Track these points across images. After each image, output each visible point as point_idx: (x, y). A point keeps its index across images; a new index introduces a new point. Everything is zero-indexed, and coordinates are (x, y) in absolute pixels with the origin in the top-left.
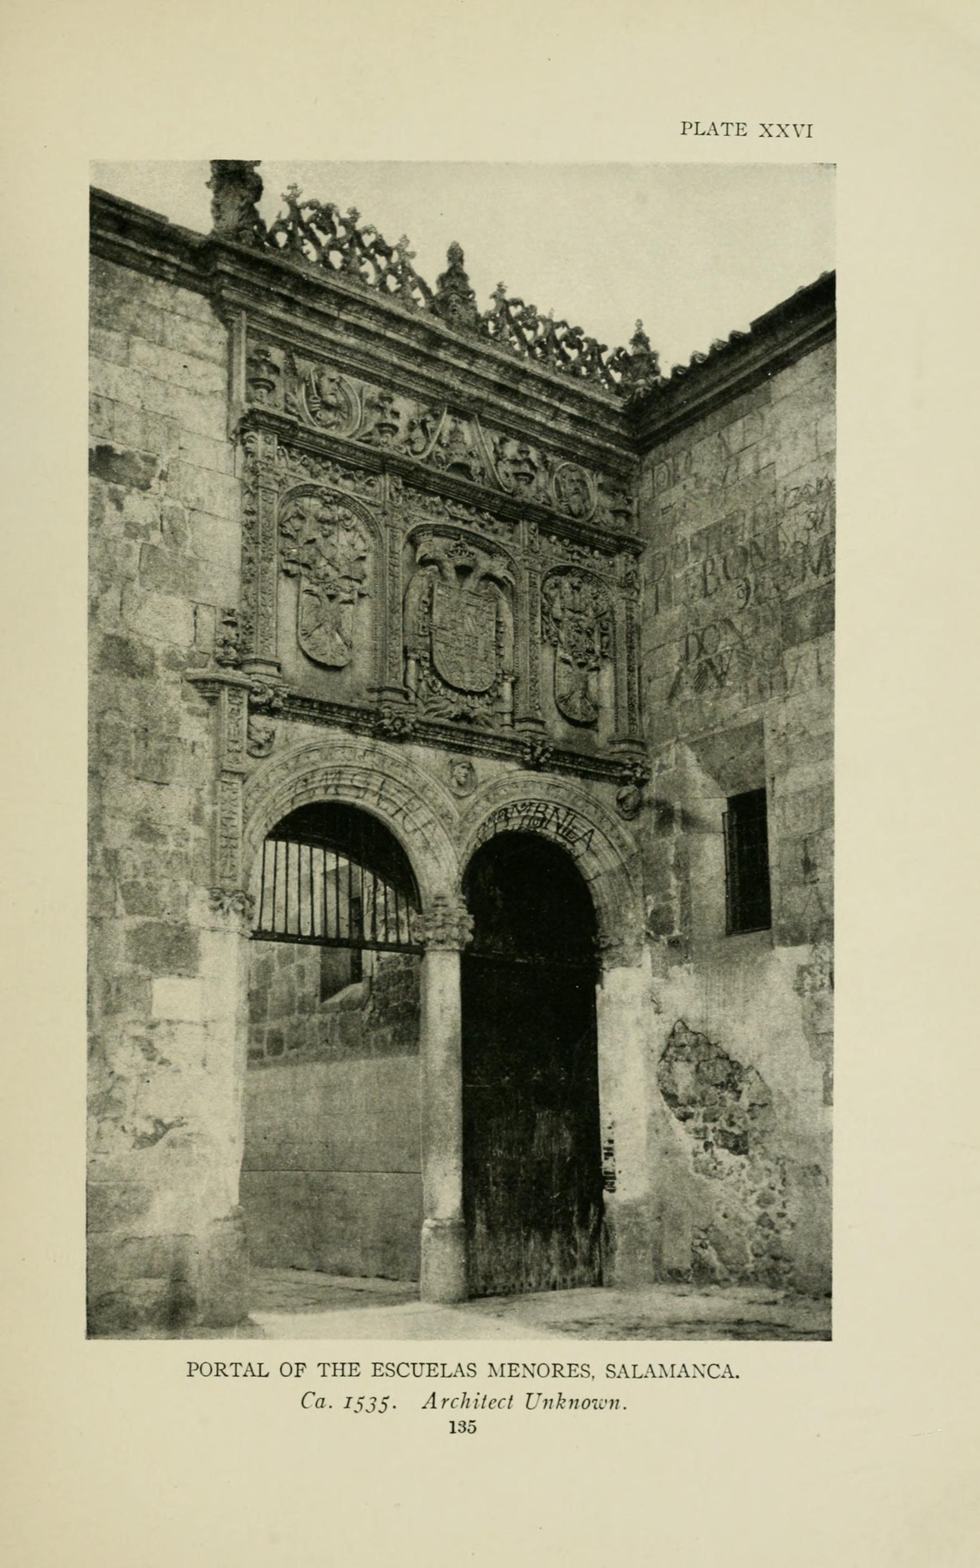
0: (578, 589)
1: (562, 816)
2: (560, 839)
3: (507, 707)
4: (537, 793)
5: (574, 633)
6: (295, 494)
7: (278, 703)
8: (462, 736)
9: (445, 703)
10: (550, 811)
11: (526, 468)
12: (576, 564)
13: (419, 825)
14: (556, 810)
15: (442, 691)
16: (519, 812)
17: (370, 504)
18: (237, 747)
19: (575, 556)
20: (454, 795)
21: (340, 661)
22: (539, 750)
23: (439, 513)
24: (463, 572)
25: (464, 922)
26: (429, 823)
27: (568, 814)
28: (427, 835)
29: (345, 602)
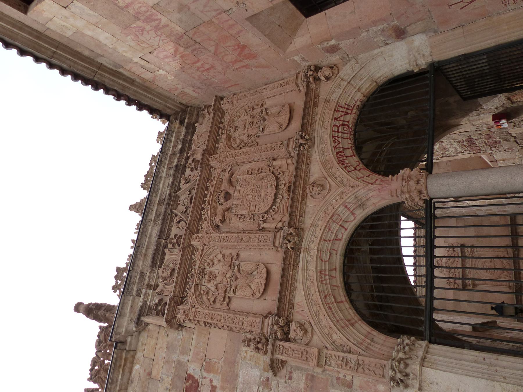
1: (340, 114)
3: (284, 162)
4: (327, 135)
5: (254, 126)
7: (281, 322)
9: (283, 202)
10: (338, 123)
13: (349, 212)
14: (336, 119)
15: (277, 205)
16: (339, 143)
18: (305, 353)
20: (328, 193)
21: (264, 271)
22: (301, 141)
25: (406, 176)
26: (346, 207)
27: (338, 111)
28: (355, 207)
29: (239, 271)
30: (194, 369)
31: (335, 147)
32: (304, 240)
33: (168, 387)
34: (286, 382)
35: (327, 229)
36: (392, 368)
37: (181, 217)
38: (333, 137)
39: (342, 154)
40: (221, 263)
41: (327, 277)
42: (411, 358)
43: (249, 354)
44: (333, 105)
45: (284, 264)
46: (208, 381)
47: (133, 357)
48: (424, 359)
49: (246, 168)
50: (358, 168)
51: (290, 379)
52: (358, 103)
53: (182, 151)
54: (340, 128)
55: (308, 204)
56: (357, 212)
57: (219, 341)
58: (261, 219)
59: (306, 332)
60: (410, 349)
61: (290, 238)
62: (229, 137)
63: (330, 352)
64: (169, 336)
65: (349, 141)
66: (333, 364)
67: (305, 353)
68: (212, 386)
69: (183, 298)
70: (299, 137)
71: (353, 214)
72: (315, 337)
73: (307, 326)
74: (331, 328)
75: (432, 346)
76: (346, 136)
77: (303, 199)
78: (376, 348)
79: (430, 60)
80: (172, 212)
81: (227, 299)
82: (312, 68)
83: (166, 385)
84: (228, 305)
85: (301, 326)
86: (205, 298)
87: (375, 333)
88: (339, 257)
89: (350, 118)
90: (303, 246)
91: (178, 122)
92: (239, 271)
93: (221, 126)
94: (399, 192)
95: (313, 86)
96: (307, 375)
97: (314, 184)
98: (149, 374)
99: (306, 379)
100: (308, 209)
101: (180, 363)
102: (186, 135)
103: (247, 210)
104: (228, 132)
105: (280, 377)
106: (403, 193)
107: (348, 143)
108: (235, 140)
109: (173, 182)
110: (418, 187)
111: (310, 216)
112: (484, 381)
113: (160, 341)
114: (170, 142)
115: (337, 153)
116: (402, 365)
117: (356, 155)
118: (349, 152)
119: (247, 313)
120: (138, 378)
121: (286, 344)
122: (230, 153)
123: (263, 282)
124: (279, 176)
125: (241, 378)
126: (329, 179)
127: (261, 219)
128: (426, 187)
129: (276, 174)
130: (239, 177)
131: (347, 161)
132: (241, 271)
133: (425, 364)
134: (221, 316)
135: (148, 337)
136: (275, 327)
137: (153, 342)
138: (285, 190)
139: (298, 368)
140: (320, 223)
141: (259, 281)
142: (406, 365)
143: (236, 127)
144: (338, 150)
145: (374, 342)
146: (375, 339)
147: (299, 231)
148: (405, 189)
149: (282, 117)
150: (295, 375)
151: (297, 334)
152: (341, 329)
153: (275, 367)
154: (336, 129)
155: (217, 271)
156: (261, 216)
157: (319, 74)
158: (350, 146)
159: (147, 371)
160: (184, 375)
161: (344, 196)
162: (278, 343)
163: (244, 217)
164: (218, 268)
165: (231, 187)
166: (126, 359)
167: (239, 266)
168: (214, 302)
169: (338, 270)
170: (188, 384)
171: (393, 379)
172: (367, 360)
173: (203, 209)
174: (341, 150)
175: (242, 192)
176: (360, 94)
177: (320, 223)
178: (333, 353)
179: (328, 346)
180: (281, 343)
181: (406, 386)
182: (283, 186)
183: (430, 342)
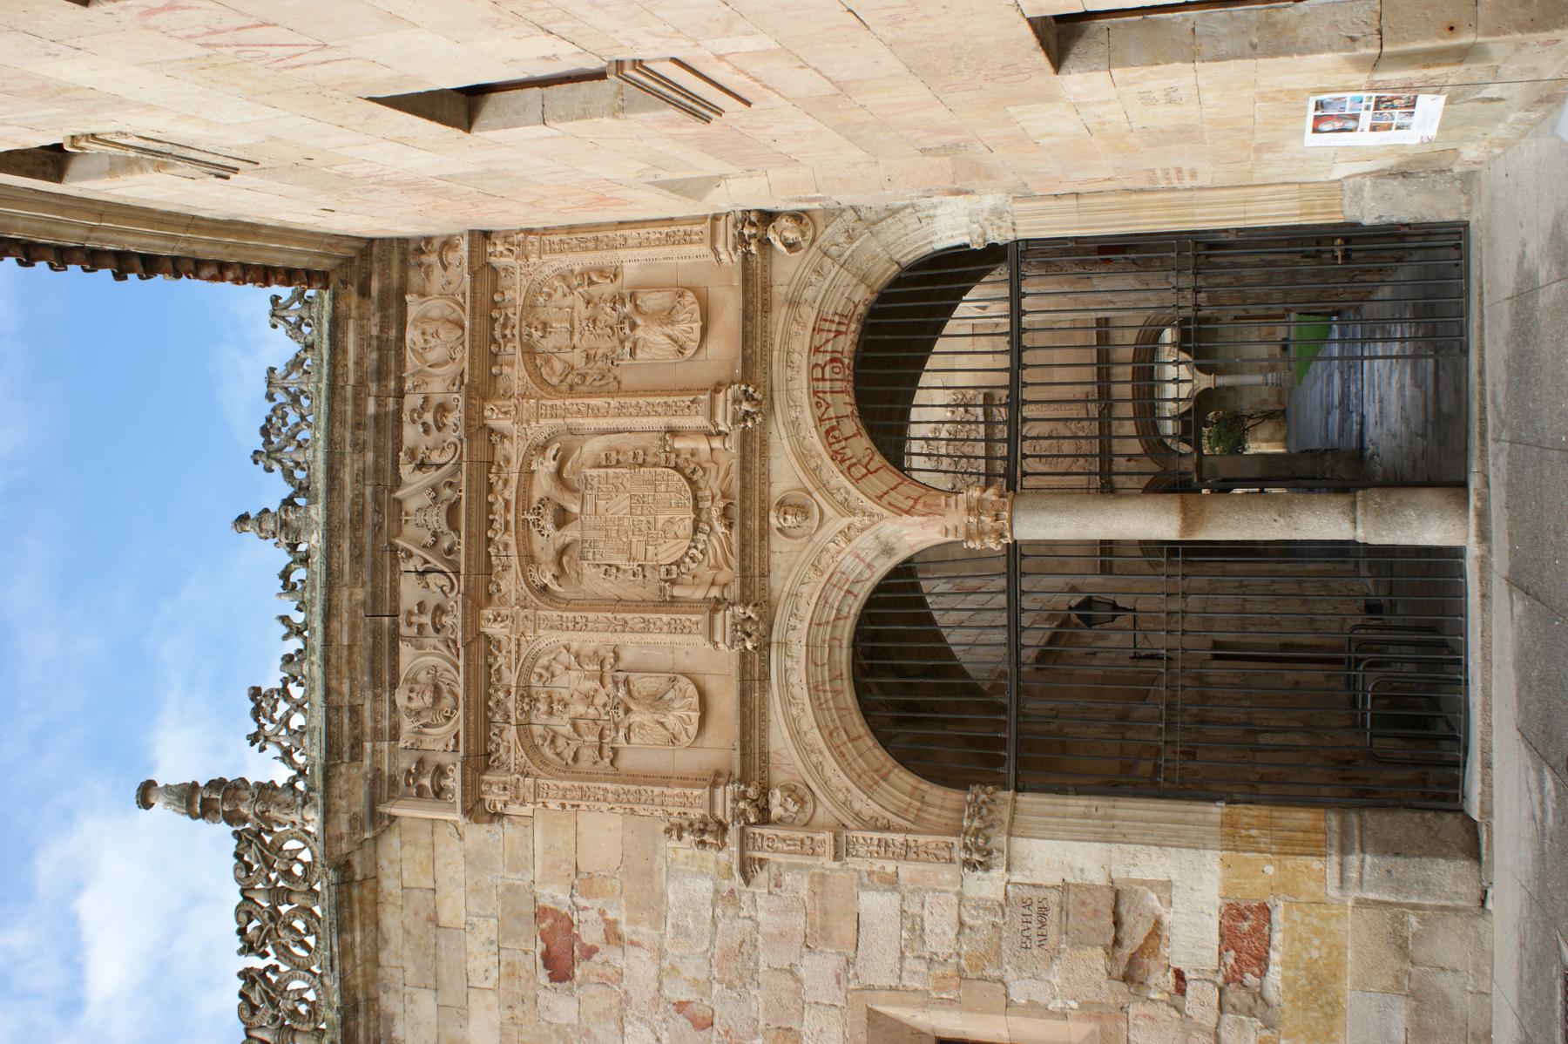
0: (545, 325)
2: (853, 326)
6: (532, 749)
7: (752, 792)
8: (749, 513)
11: (429, 417)
12: (516, 332)
14: (817, 350)
17: (518, 659)
18: (808, 842)
19: (508, 332)
20: (820, 526)
21: (691, 689)
22: (746, 406)
23: (506, 546)
24: (563, 518)
29: (629, 692)
30: (554, 894)
31: (821, 420)
32: (775, 628)
33: (494, 937)
34: (770, 893)
35: (822, 602)
36: (966, 847)
37: (426, 562)
38: (815, 393)
39: (836, 433)
40: (573, 674)
41: (829, 695)
42: (992, 826)
43: (682, 854)
44: (809, 315)
45: (742, 681)
46: (593, 915)
47: (376, 891)
48: (1011, 825)
49: (595, 446)
50: (872, 467)
51: (778, 885)
52: (861, 309)
53: (381, 374)
54: (827, 369)
55: (773, 548)
56: (877, 564)
57: (603, 833)
58: (663, 576)
59: (801, 801)
60: (990, 811)
61: (748, 628)
62: (530, 351)
63: (855, 834)
64: (468, 837)
65: (847, 399)
66: (862, 851)
67: (808, 842)
68: (606, 921)
69: (489, 755)
70: (741, 397)
71: (869, 566)
72: (820, 810)
73: (802, 790)
74: (848, 790)
75: (1020, 797)
76: (839, 385)
77: (762, 538)
78: (932, 815)
79: (1011, 237)
80: (394, 549)
81: (608, 753)
82: (753, 218)
83: (486, 934)
84: (612, 763)
85: (791, 791)
86: (548, 751)
87: (925, 786)
88: (845, 651)
89: (846, 343)
90: (774, 639)
91: (353, 289)
92: (629, 692)
93: (495, 314)
94: (961, 530)
95: (756, 262)
96: (812, 876)
97: (781, 504)
98: (434, 920)
99: (811, 882)
100: (775, 559)
101: (510, 888)
102: (384, 327)
103: (626, 556)
104: (525, 338)
105: (758, 886)
106: (969, 536)
107: (844, 404)
108: (548, 361)
109: (376, 462)
110: (997, 525)
111: (780, 573)
112: (1098, 845)
113: (440, 850)
114: (345, 351)
115: (827, 433)
116: (981, 841)
117: (863, 432)
118: (850, 427)
119: (665, 780)
120: (400, 932)
121: (767, 831)
122: (549, 403)
123: (695, 715)
124: (695, 478)
125: (671, 897)
126: (817, 496)
127: (663, 576)
128: (1011, 526)
129: (688, 471)
130: (589, 472)
131: (849, 453)
132: (635, 694)
133: (1014, 830)
134: (606, 790)
135: (402, 846)
136: (742, 805)
137: (422, 855)
138: (715, 513)
139: (791, 867)
140: (805, 589)
141: (682, 714)
142: (987, 839)
143: (545, 325)
144: (827, 425)
145: (928, 804)
146: (927, 798)
147: (766, 609)
148: (974, 529)
149: (683, 327)
150: (787, 879)
151: (786, 810)
152: (868, 790)
153: (747, 868)
154: (818, 373)
155: (566, 694)
156: (663, 570)
157: (771, 235)
158: (849, 409)
159: (423, 915)
160: (530, 910)
161: (852, 533)
162: (750, 830)
163: (618, 569)
164: (570, 683)
165: (567, 496)
166: (361, 901)
167: (626, 682)
168: (575, 758)
169: (845, 676)
170: (544, 925)
171: (966, 863)
172: (922, 839)
173: (490, 541)
174: (834, 423)
175: (601, 510)
176: (863, 286)
177: (805, 589)
178: (860, 834)
179: (847, 823)
180: (757, 830)
181: (987, 867)
182: (708, 504)
183: (1018, 790)
